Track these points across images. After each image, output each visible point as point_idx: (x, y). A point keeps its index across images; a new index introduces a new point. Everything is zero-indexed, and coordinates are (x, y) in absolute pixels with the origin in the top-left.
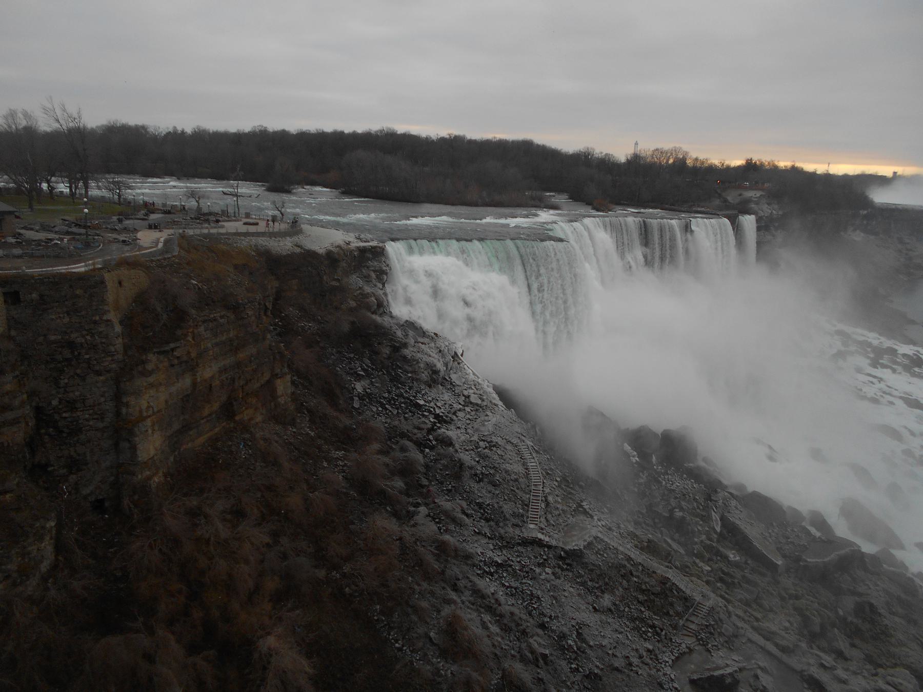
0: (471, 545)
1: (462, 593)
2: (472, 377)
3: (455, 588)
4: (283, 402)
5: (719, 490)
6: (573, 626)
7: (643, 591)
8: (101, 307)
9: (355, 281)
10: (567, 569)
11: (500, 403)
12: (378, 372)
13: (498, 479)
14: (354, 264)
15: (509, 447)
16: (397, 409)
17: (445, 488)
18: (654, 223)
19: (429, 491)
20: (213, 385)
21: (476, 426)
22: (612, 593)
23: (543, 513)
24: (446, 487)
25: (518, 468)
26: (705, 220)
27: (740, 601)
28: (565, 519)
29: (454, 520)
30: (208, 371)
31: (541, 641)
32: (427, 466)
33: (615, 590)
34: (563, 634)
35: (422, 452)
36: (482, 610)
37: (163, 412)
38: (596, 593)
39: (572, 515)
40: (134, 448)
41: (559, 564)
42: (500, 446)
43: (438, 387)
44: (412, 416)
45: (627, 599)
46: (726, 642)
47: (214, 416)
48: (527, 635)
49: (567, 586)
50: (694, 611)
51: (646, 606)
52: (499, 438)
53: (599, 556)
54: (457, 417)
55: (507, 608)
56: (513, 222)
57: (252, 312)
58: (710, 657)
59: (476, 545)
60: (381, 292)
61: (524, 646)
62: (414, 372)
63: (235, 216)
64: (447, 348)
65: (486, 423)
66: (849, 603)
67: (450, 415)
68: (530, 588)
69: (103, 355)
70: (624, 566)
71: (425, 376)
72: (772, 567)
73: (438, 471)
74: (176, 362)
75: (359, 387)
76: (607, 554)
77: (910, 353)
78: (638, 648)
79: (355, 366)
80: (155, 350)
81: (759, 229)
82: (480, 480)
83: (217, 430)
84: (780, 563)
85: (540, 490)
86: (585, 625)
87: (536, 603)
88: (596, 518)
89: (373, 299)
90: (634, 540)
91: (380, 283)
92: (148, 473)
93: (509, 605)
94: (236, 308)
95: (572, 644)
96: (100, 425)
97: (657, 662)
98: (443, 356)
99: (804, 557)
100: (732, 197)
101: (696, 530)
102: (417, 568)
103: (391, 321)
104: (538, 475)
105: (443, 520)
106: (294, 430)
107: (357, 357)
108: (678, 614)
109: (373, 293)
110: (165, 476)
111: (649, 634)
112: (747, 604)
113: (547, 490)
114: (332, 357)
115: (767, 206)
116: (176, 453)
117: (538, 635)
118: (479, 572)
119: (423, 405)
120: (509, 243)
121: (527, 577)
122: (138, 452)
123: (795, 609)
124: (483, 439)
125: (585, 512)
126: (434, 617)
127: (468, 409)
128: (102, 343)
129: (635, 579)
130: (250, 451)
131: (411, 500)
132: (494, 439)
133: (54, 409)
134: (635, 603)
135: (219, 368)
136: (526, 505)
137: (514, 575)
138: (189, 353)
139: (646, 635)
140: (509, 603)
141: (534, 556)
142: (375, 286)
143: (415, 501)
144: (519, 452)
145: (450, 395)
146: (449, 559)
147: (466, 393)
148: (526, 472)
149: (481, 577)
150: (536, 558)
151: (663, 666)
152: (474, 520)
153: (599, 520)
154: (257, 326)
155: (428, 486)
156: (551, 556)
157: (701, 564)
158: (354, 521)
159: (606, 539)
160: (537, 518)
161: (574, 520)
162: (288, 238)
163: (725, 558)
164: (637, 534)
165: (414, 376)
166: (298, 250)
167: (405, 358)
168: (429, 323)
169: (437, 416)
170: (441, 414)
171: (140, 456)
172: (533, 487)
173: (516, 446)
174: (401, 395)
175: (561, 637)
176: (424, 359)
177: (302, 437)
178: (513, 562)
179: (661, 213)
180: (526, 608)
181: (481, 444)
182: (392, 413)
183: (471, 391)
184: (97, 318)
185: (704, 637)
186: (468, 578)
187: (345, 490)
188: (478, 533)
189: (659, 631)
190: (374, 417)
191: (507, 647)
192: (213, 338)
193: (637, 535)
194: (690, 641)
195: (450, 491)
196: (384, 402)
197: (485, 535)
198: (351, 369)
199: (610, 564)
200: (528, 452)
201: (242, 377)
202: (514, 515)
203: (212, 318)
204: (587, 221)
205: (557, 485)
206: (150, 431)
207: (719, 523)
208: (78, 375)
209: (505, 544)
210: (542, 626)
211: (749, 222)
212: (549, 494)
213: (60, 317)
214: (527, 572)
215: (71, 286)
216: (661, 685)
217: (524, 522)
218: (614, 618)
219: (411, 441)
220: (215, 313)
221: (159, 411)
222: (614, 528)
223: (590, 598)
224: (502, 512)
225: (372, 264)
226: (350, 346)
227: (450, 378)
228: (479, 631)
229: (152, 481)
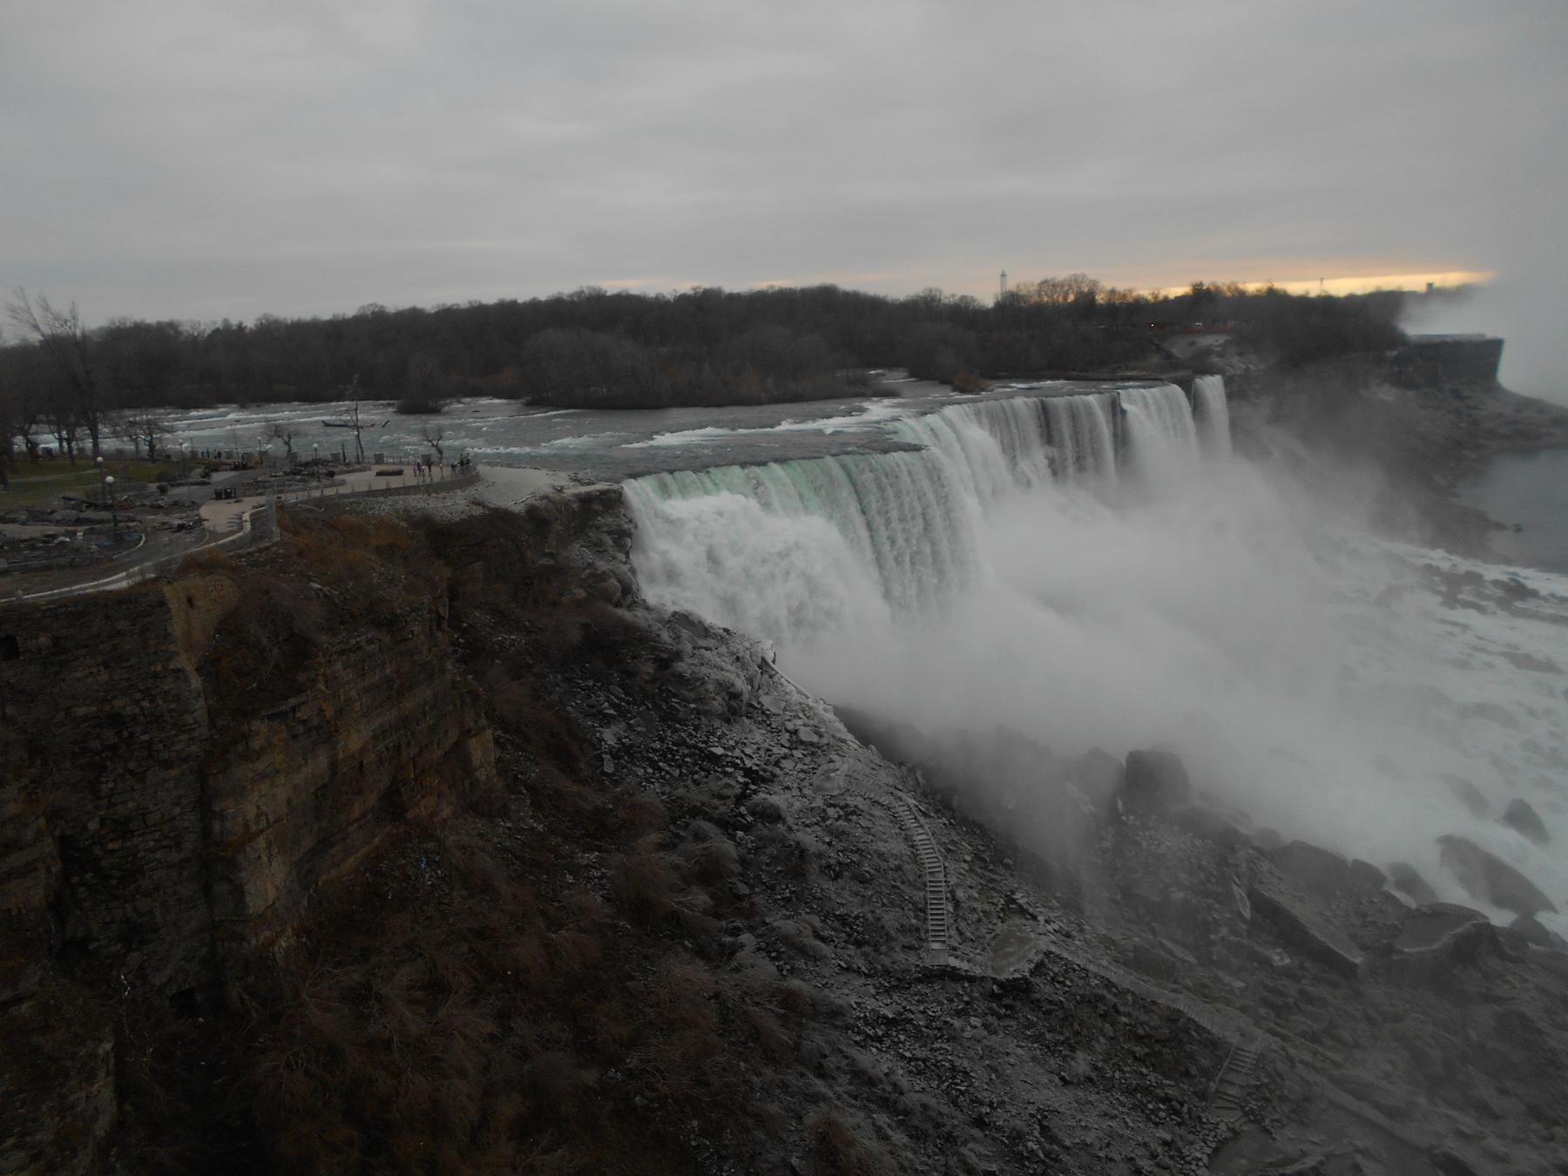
0: (838, 992)
1: (834, 1079)
2: (796, 697)
3: (821, 1072)
4: (484, 778)
5: (1238, 846)
6: (1032, 1116)
7: (1139, 1039)
8: (163, 648)
9: (578, 553)
10: (1006, 1016)
11: (849, 737)
12: (639, 707)
13: (867, 869)
14: (573, 524)
15: (877, 812)
16: (679, 767)
17: (779, 897)
18: (1059, 402)
19: (753, 904)
20: (365, 762)
21: (816, 780)
22: (1089, 1048)
23: (952, 921)
24: (780, 894)
25: (897, 846)
26: (1142, 390)
27: (1304, 1035)
28: (991, 927)
29: (803, 951)
30: (355, 739)
31: (981, 1149)
32: (743, 862)
33: (1094, 1042)
34: (1018, 1132)
35: (732, 837)
36: (873, 1106)
37: (285, 821)
38: (1061, 1051)
39: (999, 917)
40: (239, 891)
41: (991, 1009)
42: (862, 811)
43: (743, 721)
44: (707, 777)
45: (1116, 1056)
46: (1294, 1111)
47: (370, 816)
48: (956, 1142)
49: (1011, 1046)
50: (1230, 1063)
51: (1148, 1064)
52: (859, 798)
53: (1058, 986)
54: (781, 769)
55: (916, 1097)
56: (830, 425)
57: (420, 628)
58: (1271, 1141)
59: (846, 991)
60: (625, 568)
61: (953, 1161)
62: (698, 700)
63: (358, 463)
64: (748, 652)
65: (832, 775)
67: (770, 768)
68: (950, 1057)
69: (174, 732)
70: (1102, 999)
72: (1348, 969)
73: (764, 867)
74: (301, 729)
75: (609, 736)
76: (1071, 981)
77: (1505, 578)
78: (1147, 1140)
79: (598, 701)
80: (264, 713)
81: (1230, 396)
82: (838, 876)
83: (377, 840)
84: (1358, 960)
85: (941, 882)
86: (1052, 1111)
87: (962, 1082)
88: (1041, 919)
89: (614, 581)
90: (1110, 950)
91: (620, 551)
92: (268, 933)
93: (917, 1092)
94: (391, 624)
95: (1035, 1147)
96: (175, 857)
97: (1182, 1162)
98: (744, 667)
99: (1398, 947)
100: (1179, 348)
101: (1211, 919)
102: (751, 1044)
103: (649, 617)
104: (933, 855)
105: (784, 952)
106: (509, 825)
107: (599, 684)
108: (1205, 1072)
109: (612, 571)
110: (297, 934)
111: (1162, 1114)
112: (1314, 1038)
113: (953, 880)
114: (557, 689)
115: (1237, 358)
116: (311, 891)
117: (974, 1139)
118: (858, 1038)
119: (722, 755)
120: (829, 460)
121: (941, 1037)
122: (248, 899)
124: (832, 802)
125: (1022, 911)
126: (793, 1128)
127: (798, 754)
128: (170, 711)
129: (1125, 1020)
130: (439, 872)
131: (724, 923)
132: (851, 801)
133: (92, 837)
134: (1129, 1061)
135: (374, 730)
136: (921, 910)
137: (919, 1036)
138: (321, 710)
139: (1157, 1116)
140: (917, 1088)
141: (947, 998)
142: (614, 558)
143: (730, 926)
144: (895, 819)
145: (764, 732)
146: (804, 1021)
147: (790, 726)
148: (912, 852)
149: (862, 1047)
150: (951, 1001)
151: (1194, 1167)
152: (836, 947)
153: (1047, 922)
154: (430, 650)
155: (749, 896)
156: (976, 995)
157: (1227, 979)
158: (633, 974)
159: (1065, 955)
160: (943, 931)
161: (1005, 926)
162: (459, 492)
163: (1267, 962)
164: (1114, 938)
165: (700, 708)
166: (478, 511)
167: (680, 676)
168: (712, 616)
169: (748, 772)
170: (755, 768)
171: (251, 904)
172: (928, 878)
173: (889, 809)
174: (682, 743)
175: (1015, 1139)
176: (713, 676)
177: (523, 835)
178: (913, 1013)
179: (1069, 385)
180: (947, 1094)
181: (831, 812)
182: (672, 775)
183: (799, 722)
184: (159, 668)
185: (1256, 1107)
186: (840, 1051)
187: (609, 921)
188: (848, 969)
189: (1178, 1106)
190: (642, 787)
191: (925, 1168)
192: (358, 680)
193: (1113, 941)
194: (1232, 1118)
195: (788, 900)
196: (656, 758)
197: (858, 972)
198: (592, 707)
199: (1078, 997)
200: (910, 817)
201: (412, 743)
202: (903, 930)
203: (353, 645)
204: (950, 411)
205: (967, 868)
206: (265, 858)
207: (1248, 903)
208: (131, 772)
209: (894, 983)
210: (980, 1122)
211: (1212, 386)
212: (957, 885)
213: (92, 673)
214: (939, 1029)
215: (107, 617)
217: (921, 939)
218: (1098, 1093)
219: (710, 820)
220: (358, 636)
221: (277, 820)
222: (1074, 933)
223: (1053, 1063)
224: (883, 927)
225: (603, 521)
226: (585, 667)
227: (759, 703)
228: (874, 1145)
229: (276, 948)
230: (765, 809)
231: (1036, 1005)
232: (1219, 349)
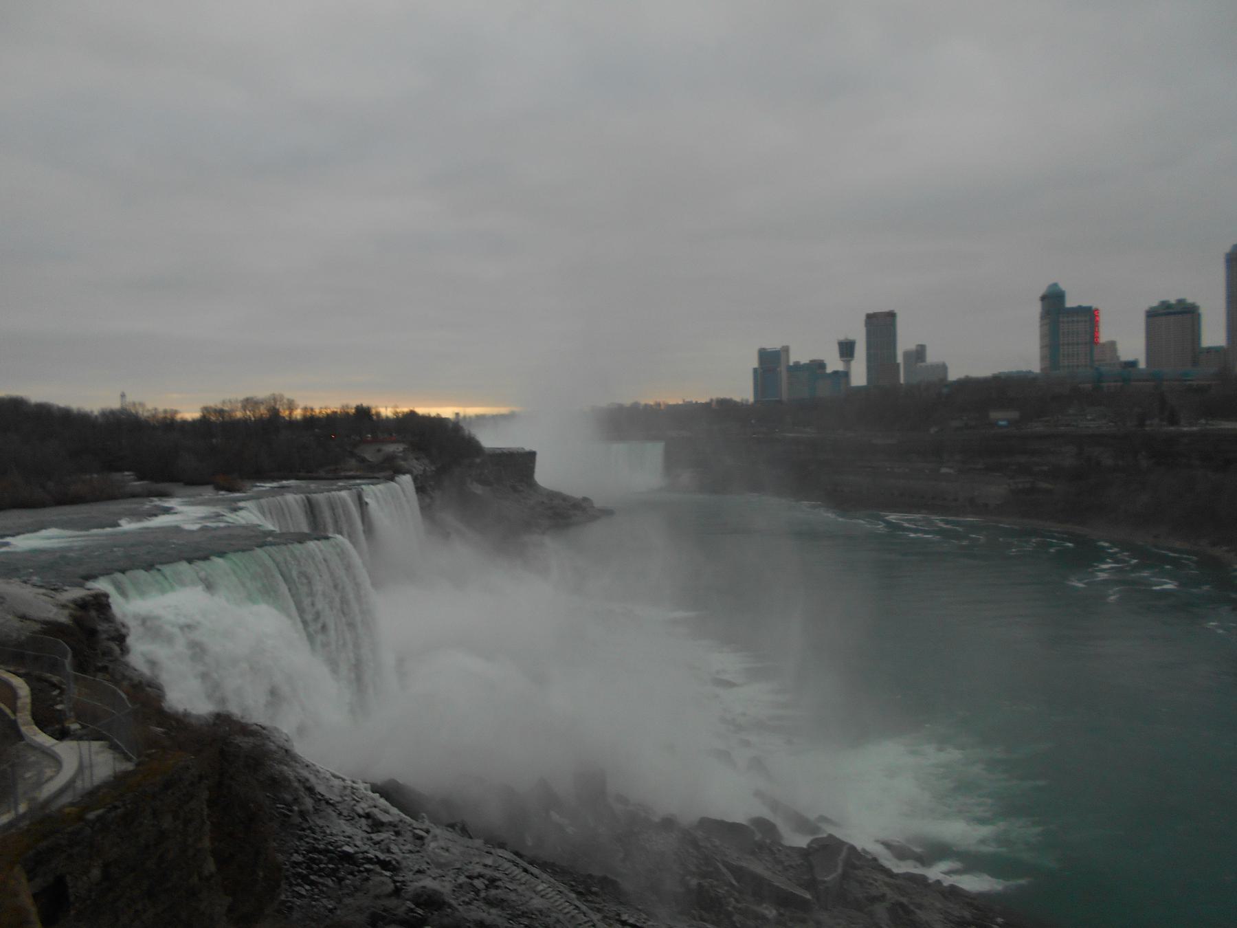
18: (320, 497)
26: (372, 486)
71: (309, 803)
100: (370, 454)
115: (415, 461)
166: (37, 627)
211: (406, 479)
232: (401, 454)
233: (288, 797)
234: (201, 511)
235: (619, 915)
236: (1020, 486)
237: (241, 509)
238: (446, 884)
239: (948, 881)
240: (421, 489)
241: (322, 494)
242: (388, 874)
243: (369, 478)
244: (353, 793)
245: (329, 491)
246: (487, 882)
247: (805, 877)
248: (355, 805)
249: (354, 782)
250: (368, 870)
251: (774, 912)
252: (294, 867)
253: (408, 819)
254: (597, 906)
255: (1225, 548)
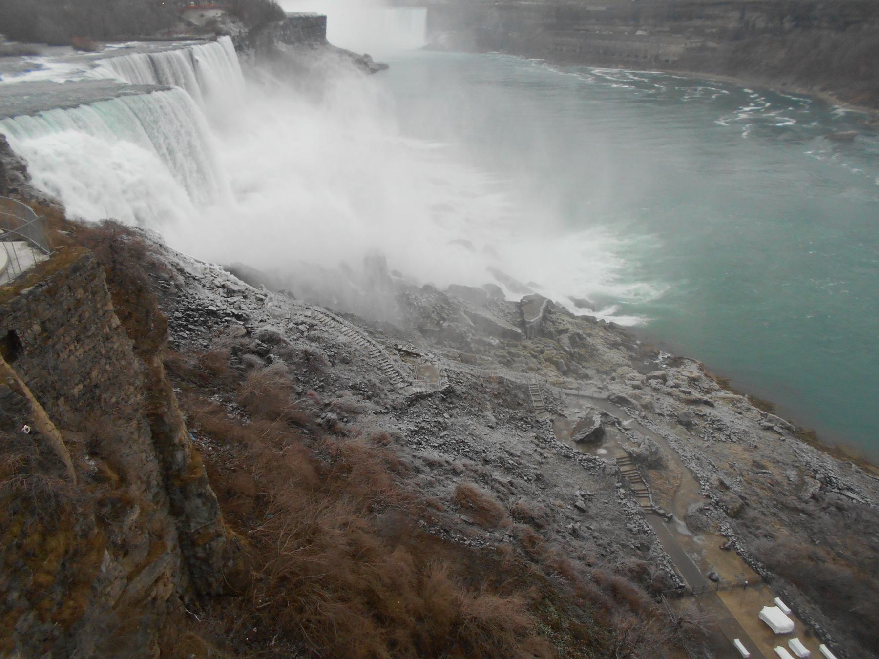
18: (159, 56)
66: (565, 339)
71: (181, 279)
72: (516, 336)
115: (232, 25)
123: (546, 360)
150: (429, 410)
151: (554, 443)
163: (490, 344)
209: (400, 412)
211: (226, 40)
216: (568, 457)
230: (271, 336)
231: (458, 396)
232: (220, 19)
233: (166, 276)
234: (66, 68)
235: (396, 345)
236: (694, 45)
237: (98, 66)
238: (280, 328)
239: (608, 320)
240: (239, 48)
241: (160, 53)
242: (241, 323)
243: (196, 39)
244: (211, 272)
245: (166, 50)
246: (308, 327)
247: (519, 320)
248: (213, 280)
249: (211, 265)
250: (226, 321)
251: (497, 341)
252: (176, 321)
253: (252, 288)
254: (382, 340)
255: (830, 93)
